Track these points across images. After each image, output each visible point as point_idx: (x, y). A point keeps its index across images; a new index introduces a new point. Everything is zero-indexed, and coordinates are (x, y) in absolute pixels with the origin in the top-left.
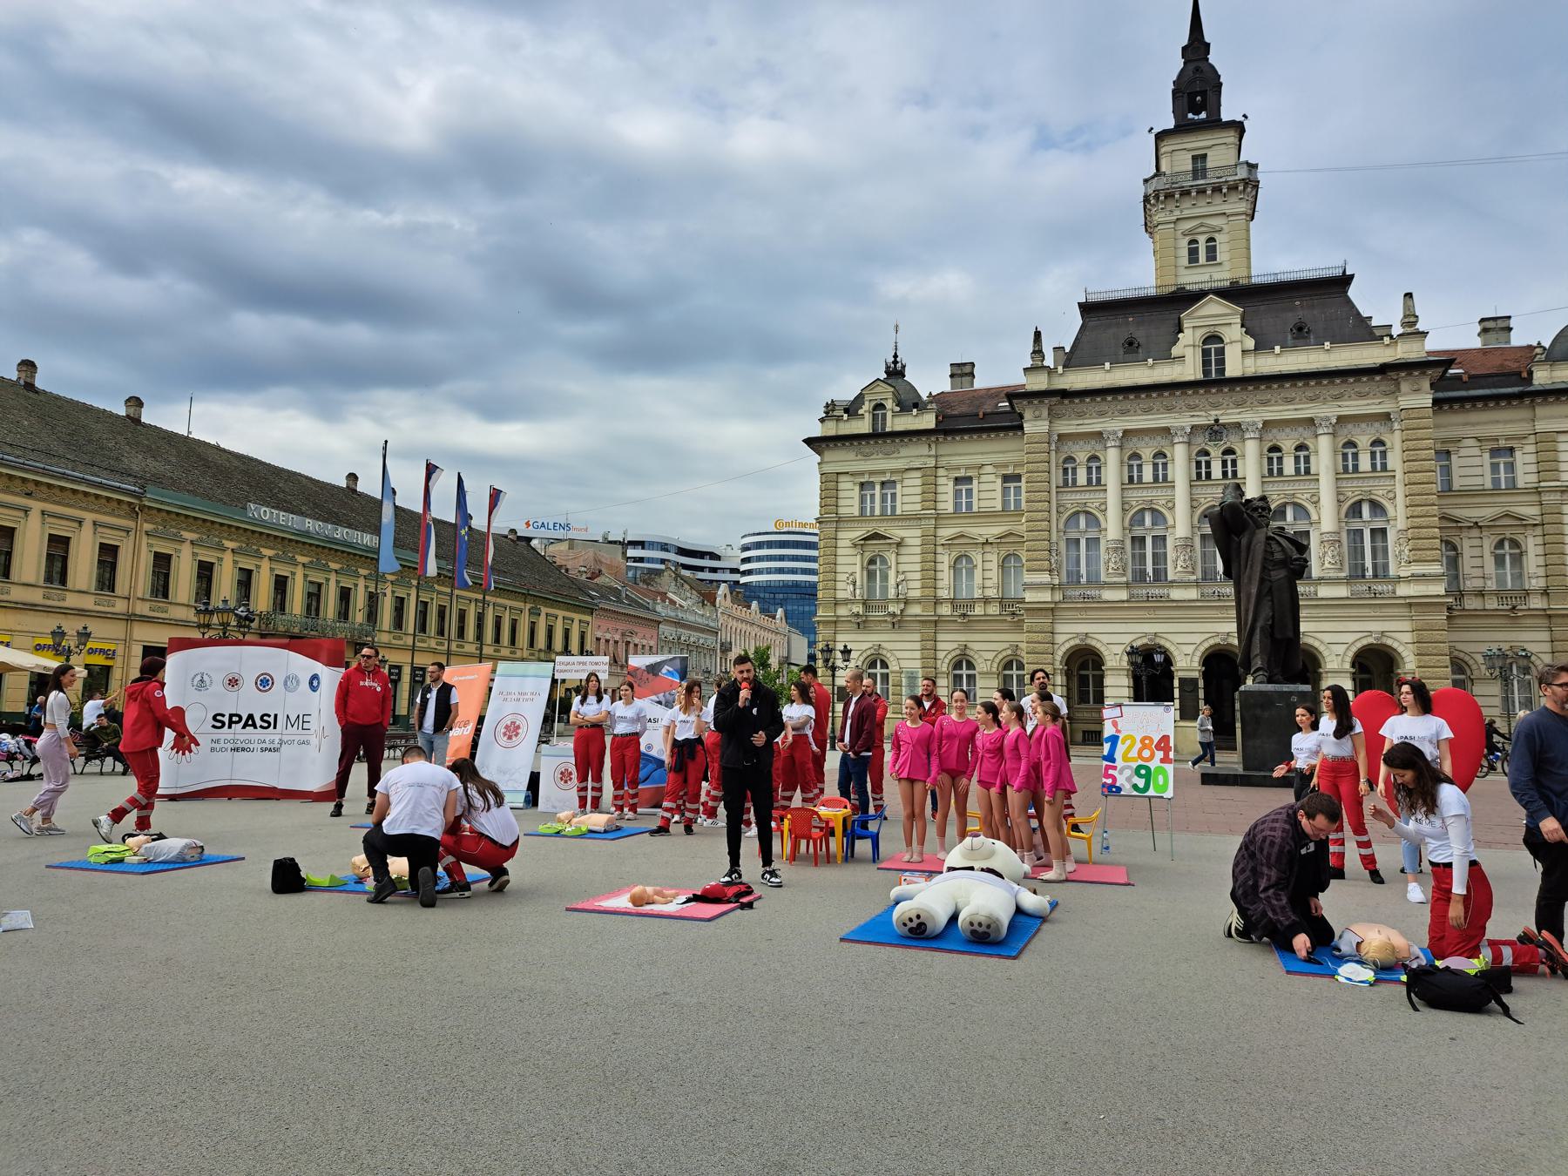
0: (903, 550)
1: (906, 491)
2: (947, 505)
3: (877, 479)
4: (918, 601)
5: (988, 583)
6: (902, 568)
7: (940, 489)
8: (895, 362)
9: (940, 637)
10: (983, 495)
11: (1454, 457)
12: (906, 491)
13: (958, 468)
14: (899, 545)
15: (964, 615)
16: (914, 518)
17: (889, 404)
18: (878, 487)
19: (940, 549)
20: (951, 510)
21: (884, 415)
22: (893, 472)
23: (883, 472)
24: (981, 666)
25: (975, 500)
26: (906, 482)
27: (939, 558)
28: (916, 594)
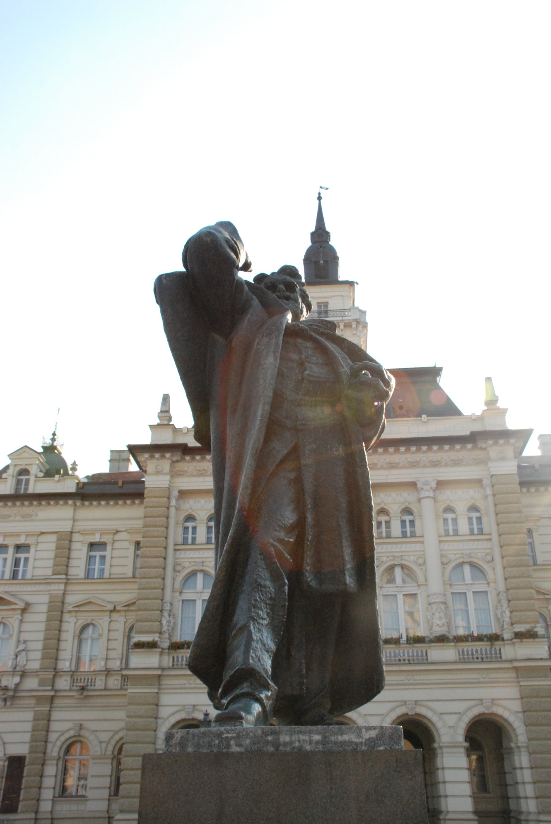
0: (28, 617)
1: (39, 555)
2: (78, 568)
3: (11, 542)
4: (35, 673)
5: (112, 654)
6: (24, 637)
7: (74, 554)
8: (53, 440)
9: (55, 715)
10: (115, 562)
11: (535, 534)
12: (39, 555)
13: (92, 533)
14: (24, 611)
15: (83, 689)
16: (46, 581)
17: (34, 470)
18: (11, 550)
19: (66, 617)
20: (82, 575)
21: (28, 481)
22: (28, 535)
23: (18, 535)
24: (95, 749)
25: (107, 567)
26: (40, 547)
27: (65, 626)
28: (35, 665)
